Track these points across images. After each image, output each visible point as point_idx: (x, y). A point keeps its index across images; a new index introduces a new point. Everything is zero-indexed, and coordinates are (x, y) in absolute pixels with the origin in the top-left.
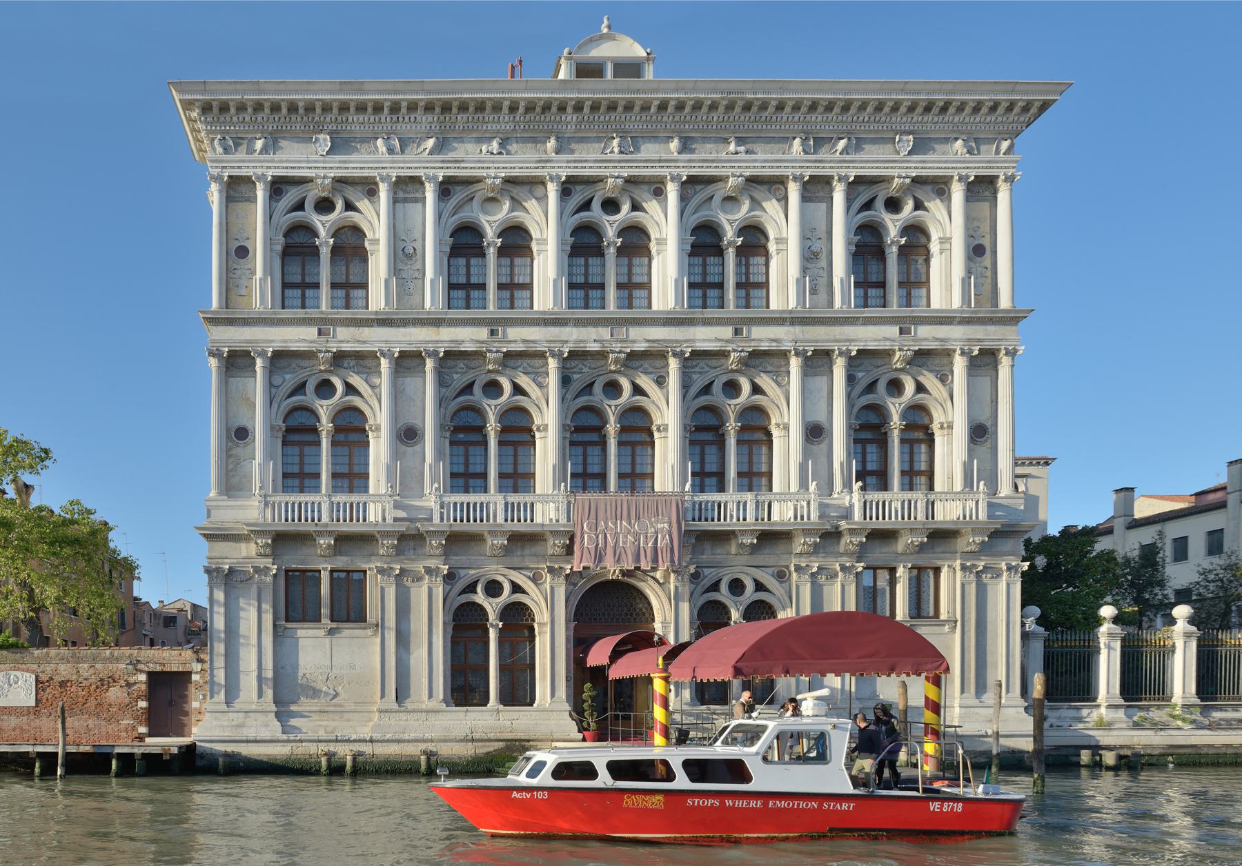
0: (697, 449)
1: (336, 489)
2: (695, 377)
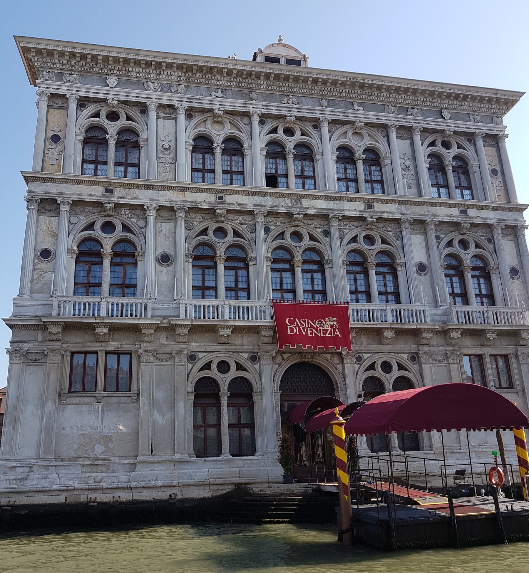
0: (352, 276)
1: (111, 294)
2: (346, 232)
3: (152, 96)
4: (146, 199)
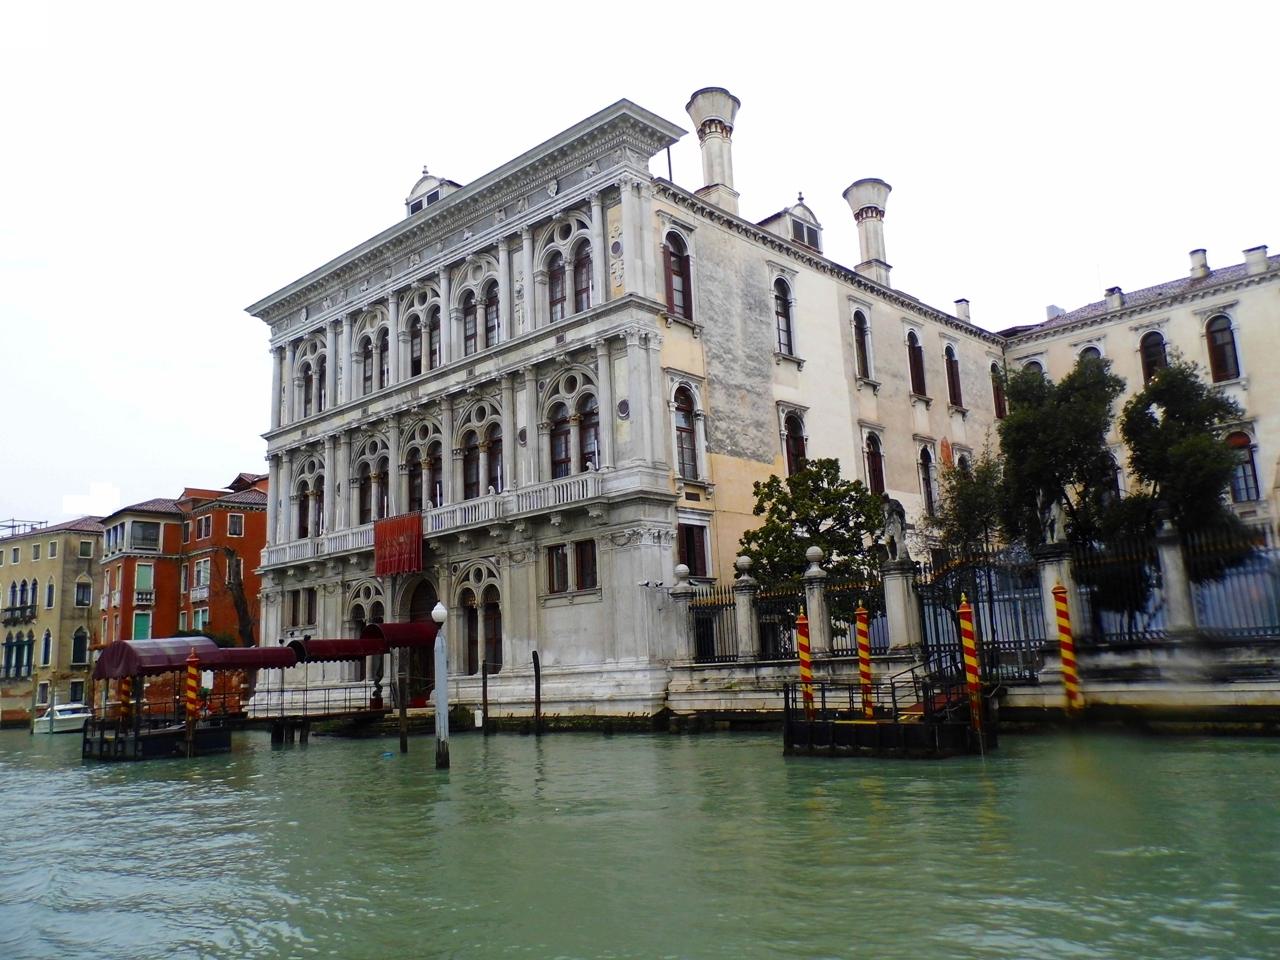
3: (324, 317)
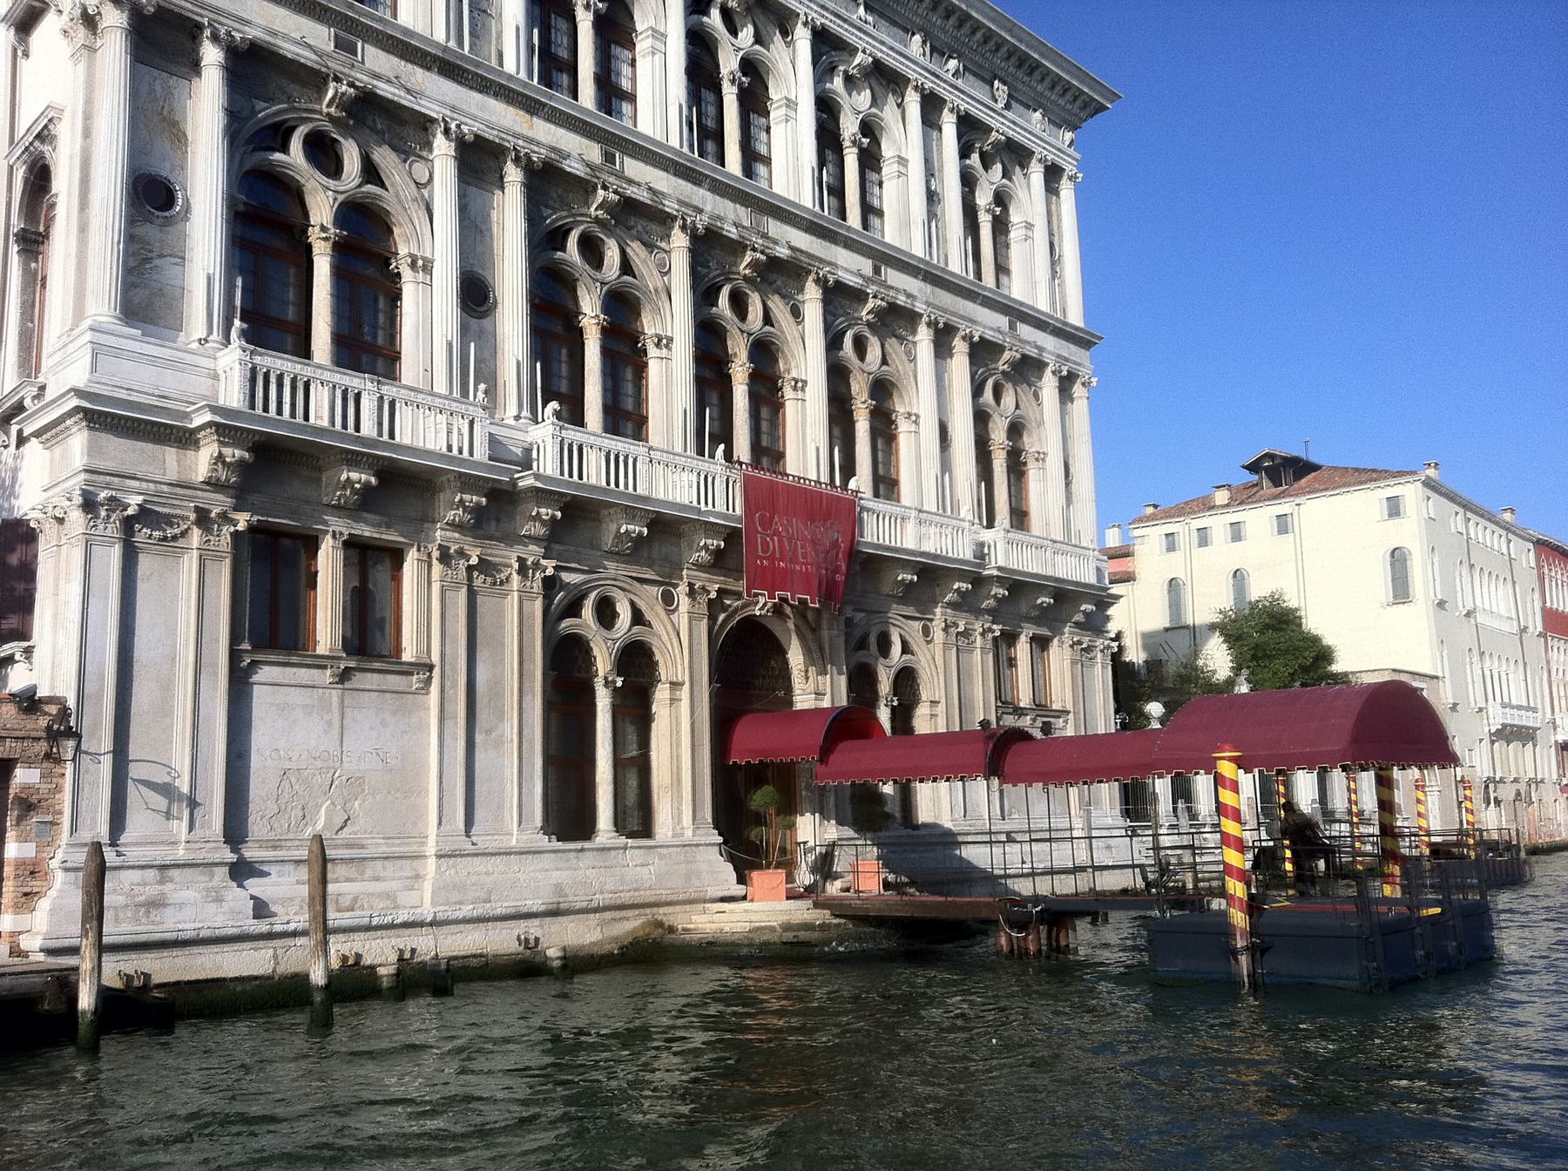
4: (443, 104)
